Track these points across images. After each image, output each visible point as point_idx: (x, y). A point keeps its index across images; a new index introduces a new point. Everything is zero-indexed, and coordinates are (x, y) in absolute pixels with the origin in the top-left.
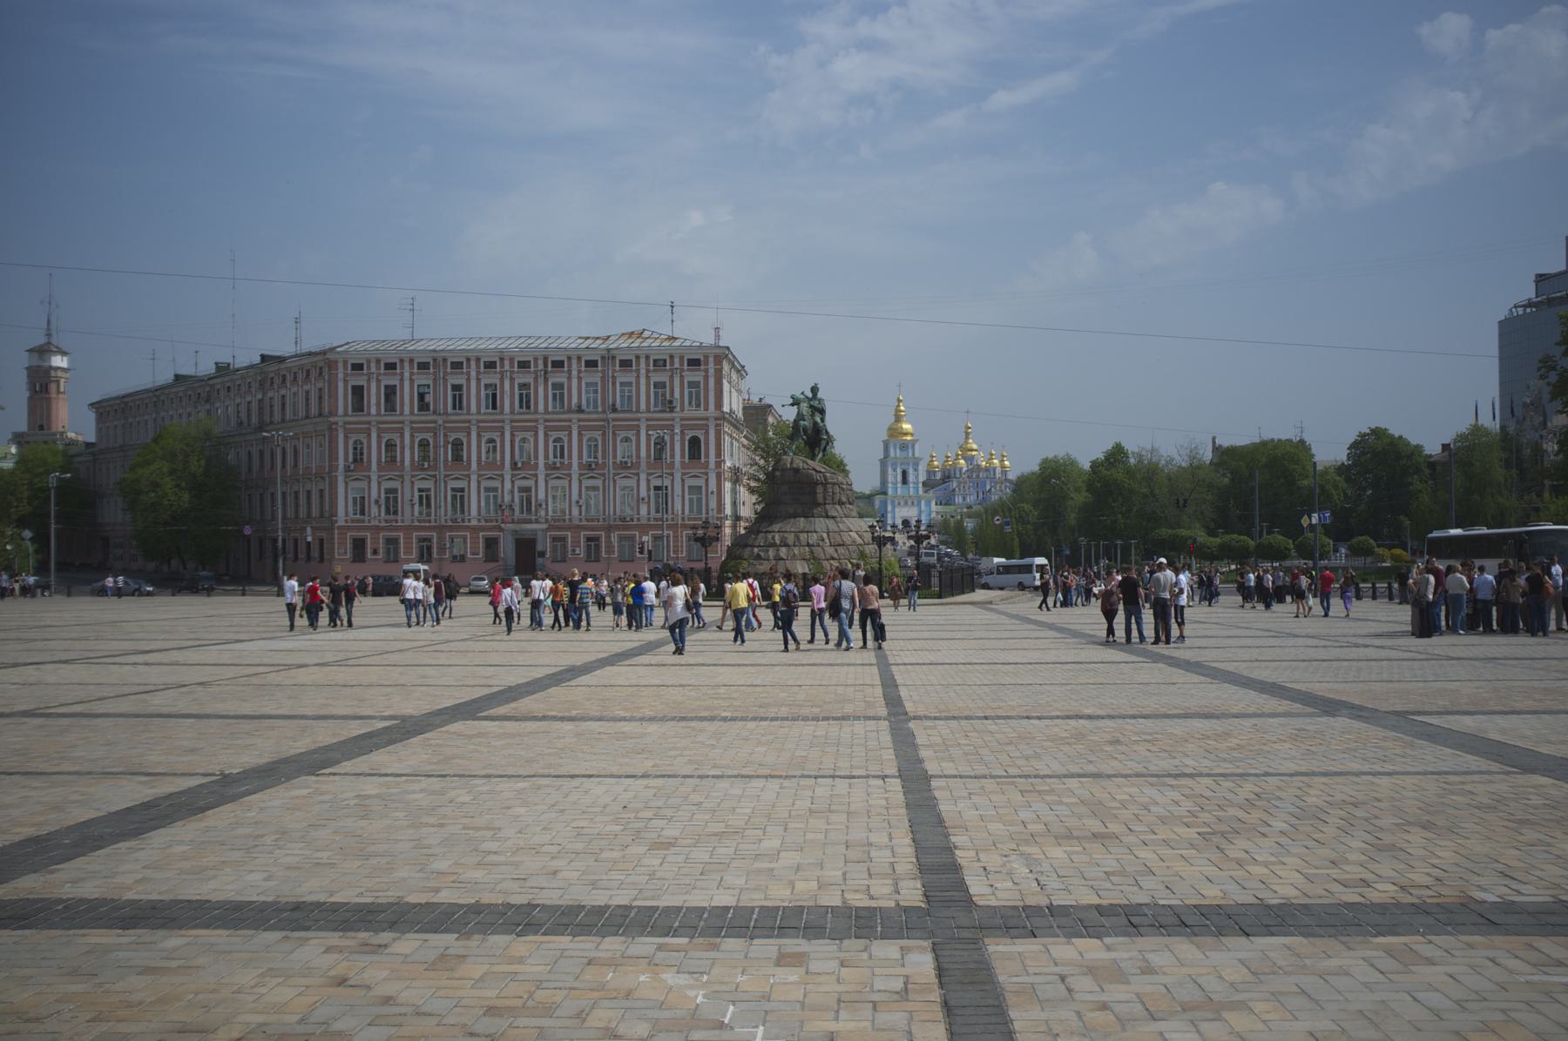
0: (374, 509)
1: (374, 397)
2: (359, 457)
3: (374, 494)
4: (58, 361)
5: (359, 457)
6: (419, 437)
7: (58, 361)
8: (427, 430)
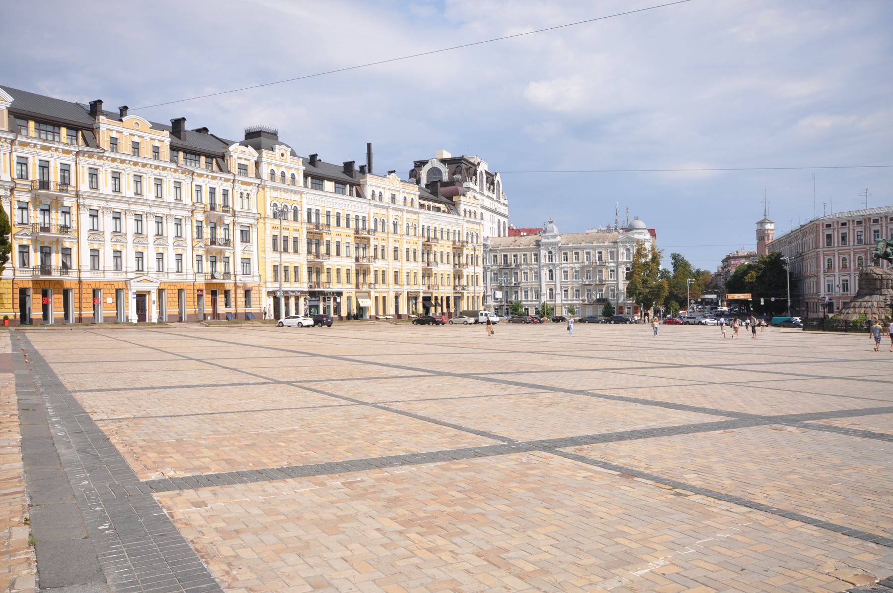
0: (837, 289)
1: (836, 238)
2: (830, 267)
3: (837, 283)
4: (768, 226)
5: (830, 267)
6: (858, 255)
7: (768, 226)
8: (861, 252)
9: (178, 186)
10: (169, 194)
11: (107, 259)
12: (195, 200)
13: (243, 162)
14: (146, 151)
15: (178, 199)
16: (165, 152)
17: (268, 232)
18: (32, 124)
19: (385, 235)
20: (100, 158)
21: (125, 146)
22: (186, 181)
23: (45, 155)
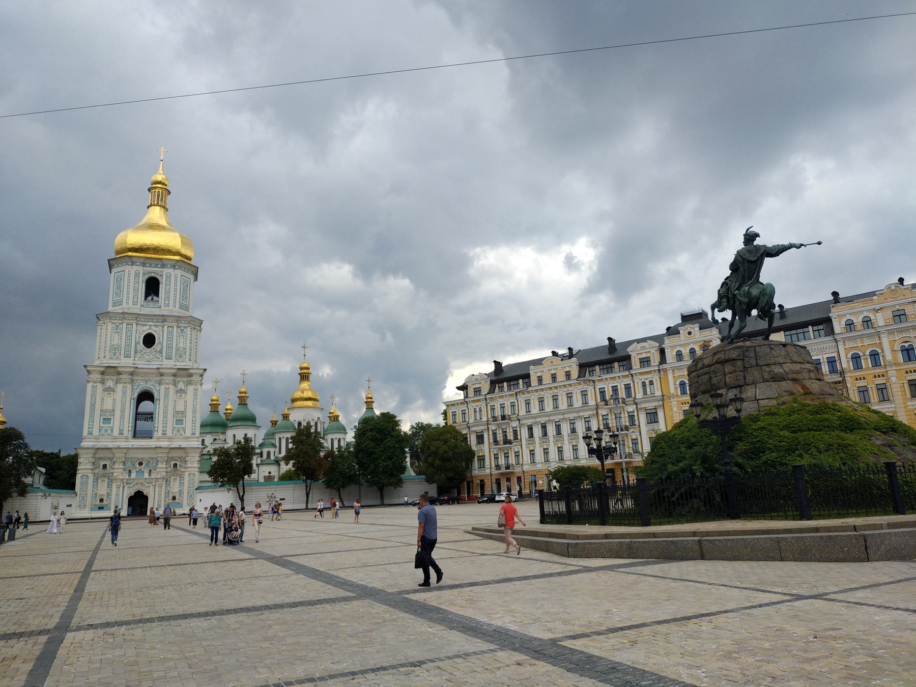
9: (584, 394)
10: (578, 402)
11: (539, 456)
12: (599, 400)
13: (644, 356)
14: (561, 377)
15: (585, 403)
16: (575, 373)
17: (675, 409)
18: (505, 384)
19: (878, 371)
20: (529, 392)
21: (547, 380)
22: (590, 389)
23: (501, 401)
